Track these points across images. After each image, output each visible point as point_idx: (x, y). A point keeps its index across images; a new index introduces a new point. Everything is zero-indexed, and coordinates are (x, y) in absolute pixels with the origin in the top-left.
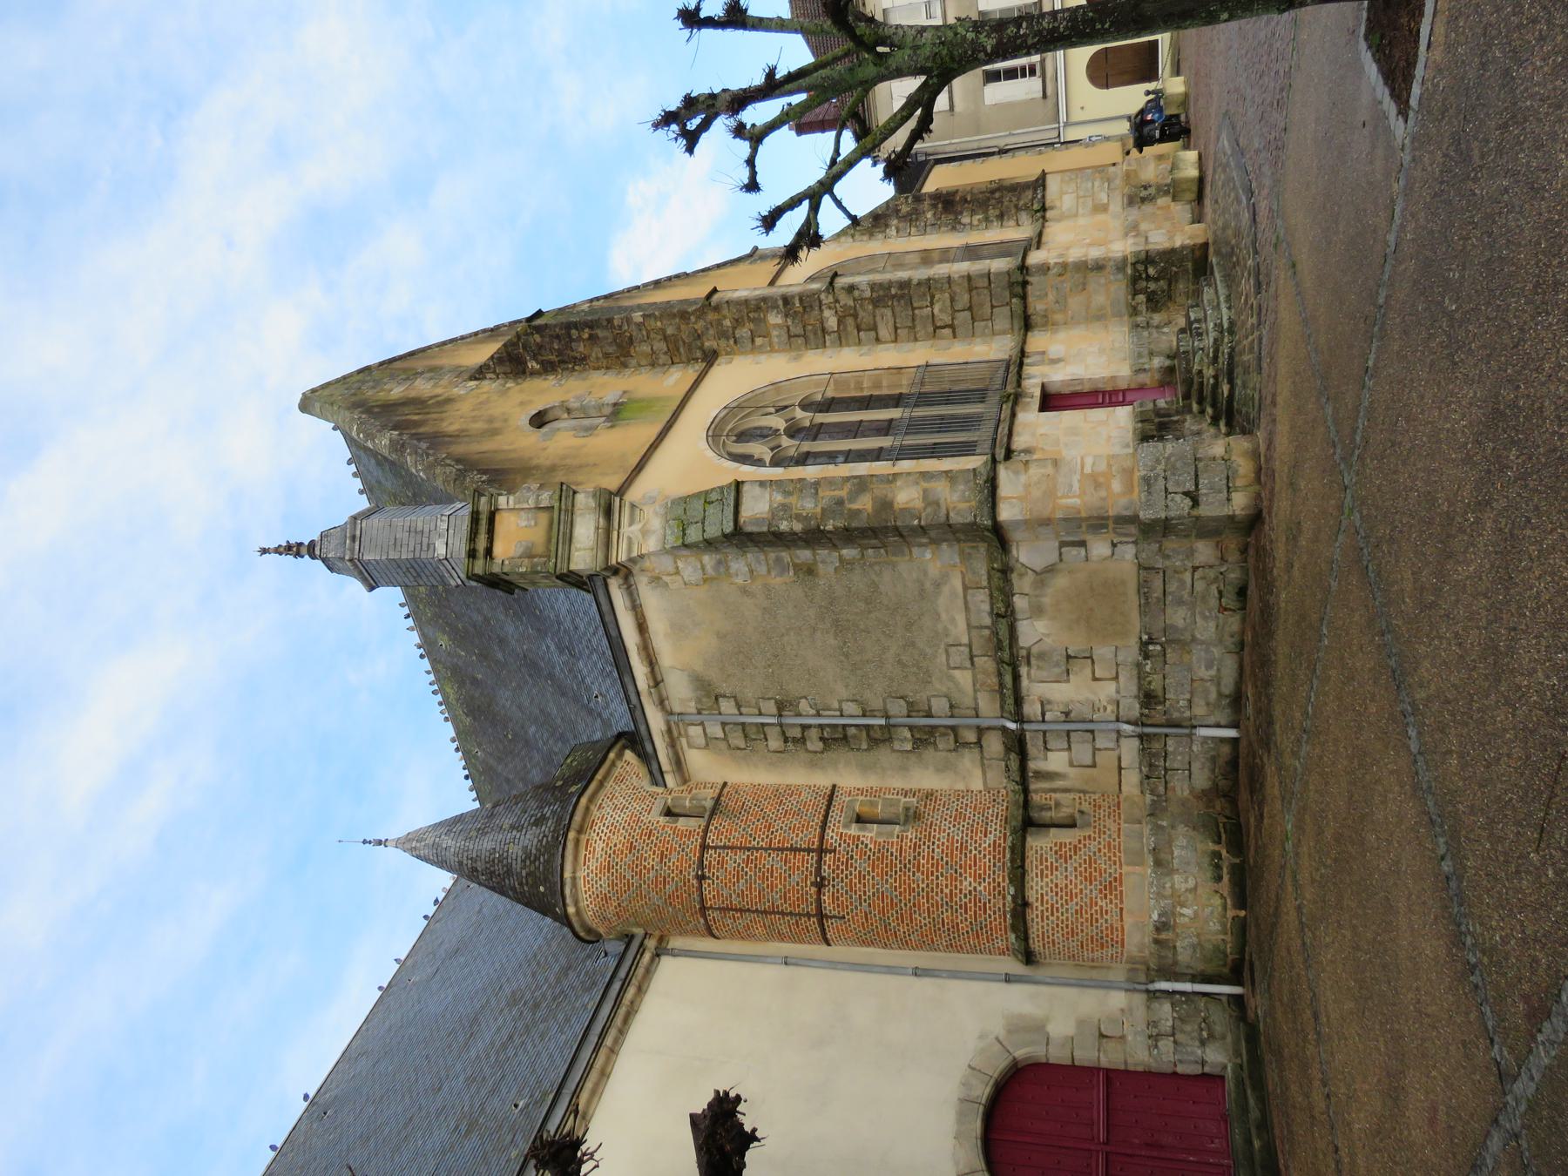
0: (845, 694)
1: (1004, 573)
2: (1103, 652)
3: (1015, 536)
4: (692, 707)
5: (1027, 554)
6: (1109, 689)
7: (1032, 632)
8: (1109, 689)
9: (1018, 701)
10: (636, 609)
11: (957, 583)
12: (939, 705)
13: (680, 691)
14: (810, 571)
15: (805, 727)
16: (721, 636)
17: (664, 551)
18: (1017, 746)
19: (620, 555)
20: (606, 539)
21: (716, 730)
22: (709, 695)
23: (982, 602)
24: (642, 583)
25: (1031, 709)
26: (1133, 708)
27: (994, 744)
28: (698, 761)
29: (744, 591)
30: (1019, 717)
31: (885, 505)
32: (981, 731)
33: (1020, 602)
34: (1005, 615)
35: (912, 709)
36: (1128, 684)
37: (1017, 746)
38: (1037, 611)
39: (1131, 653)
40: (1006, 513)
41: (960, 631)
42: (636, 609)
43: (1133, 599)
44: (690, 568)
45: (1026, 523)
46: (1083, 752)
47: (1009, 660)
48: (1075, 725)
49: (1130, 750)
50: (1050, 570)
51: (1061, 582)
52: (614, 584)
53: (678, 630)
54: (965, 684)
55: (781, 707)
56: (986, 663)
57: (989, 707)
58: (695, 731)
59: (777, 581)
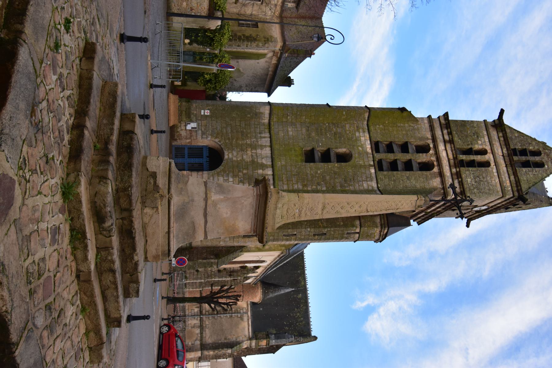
0: (223, 319)
1: (201, 340)
2: (190, 328)
3: (199, 346)
4: (245, 315)
5: (198, 342)
6: (189, 323)
7: (198, 331)
8: (189, 323)
9: (200, 320)
10: (249, 332)
11: (207, 338)
12: (211, 318)
13: (245, 318)
14: (225, 339)
15: (229, 313)
16: (238, 328)
17: (243, 342)
18: (201, 312)
19: (249, 342)
20: (251, 344)
21: (242, 311)
22: (242, 318)
23: (204, 335)
24: (247, 336)
25: (199, 319)
26: (187, 320)
27: (204, 312)
28: (245, 306)
29: (234, 335)
30: (201, 318)
31: (214, 352)
32: (205, 314)
33: (199, 335)
34: (201, 333)
35: (214, 317)
36: (187, 323)
37: (201, 312)
38: (197, 334)
39: (187, 328)
40: (200, 352)
41: (207, 330)
42: (249, 332)
43: (186, 336)
44: (241, 339)
45: (198, 351)
46: (193, 312)
47: (201, 327)
48: (194, 316)
49: (187, 313)
50: (196, 340)
51: (194, 339)
52: (251, 337)
53: (244, 328)
54: (207, 322)
55: (232, 316)
56: (204, 325)
57: (204, 317)
58: (244, 311)
59: (230, 337)
